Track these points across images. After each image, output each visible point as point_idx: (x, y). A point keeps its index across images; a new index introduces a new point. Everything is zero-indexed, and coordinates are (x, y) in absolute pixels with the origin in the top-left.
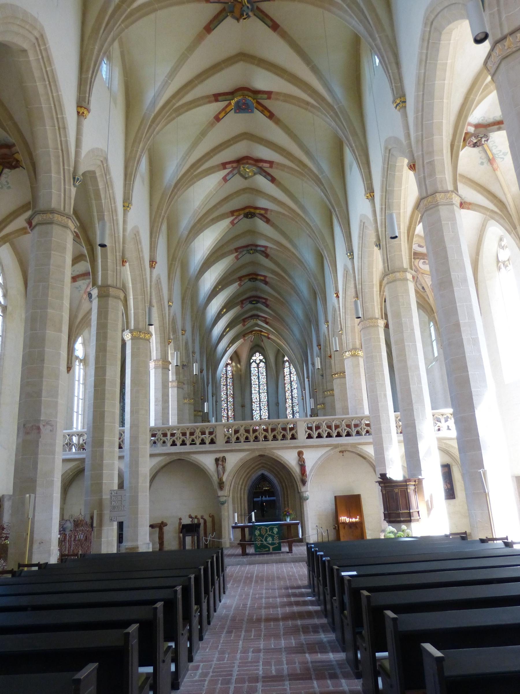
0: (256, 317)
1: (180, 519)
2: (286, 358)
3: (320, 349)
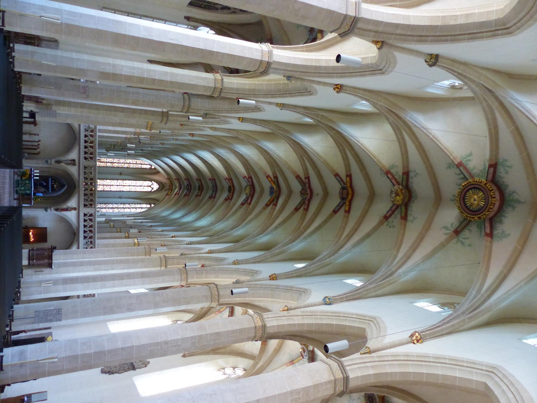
1: (38, 135)
2: (153, 205)
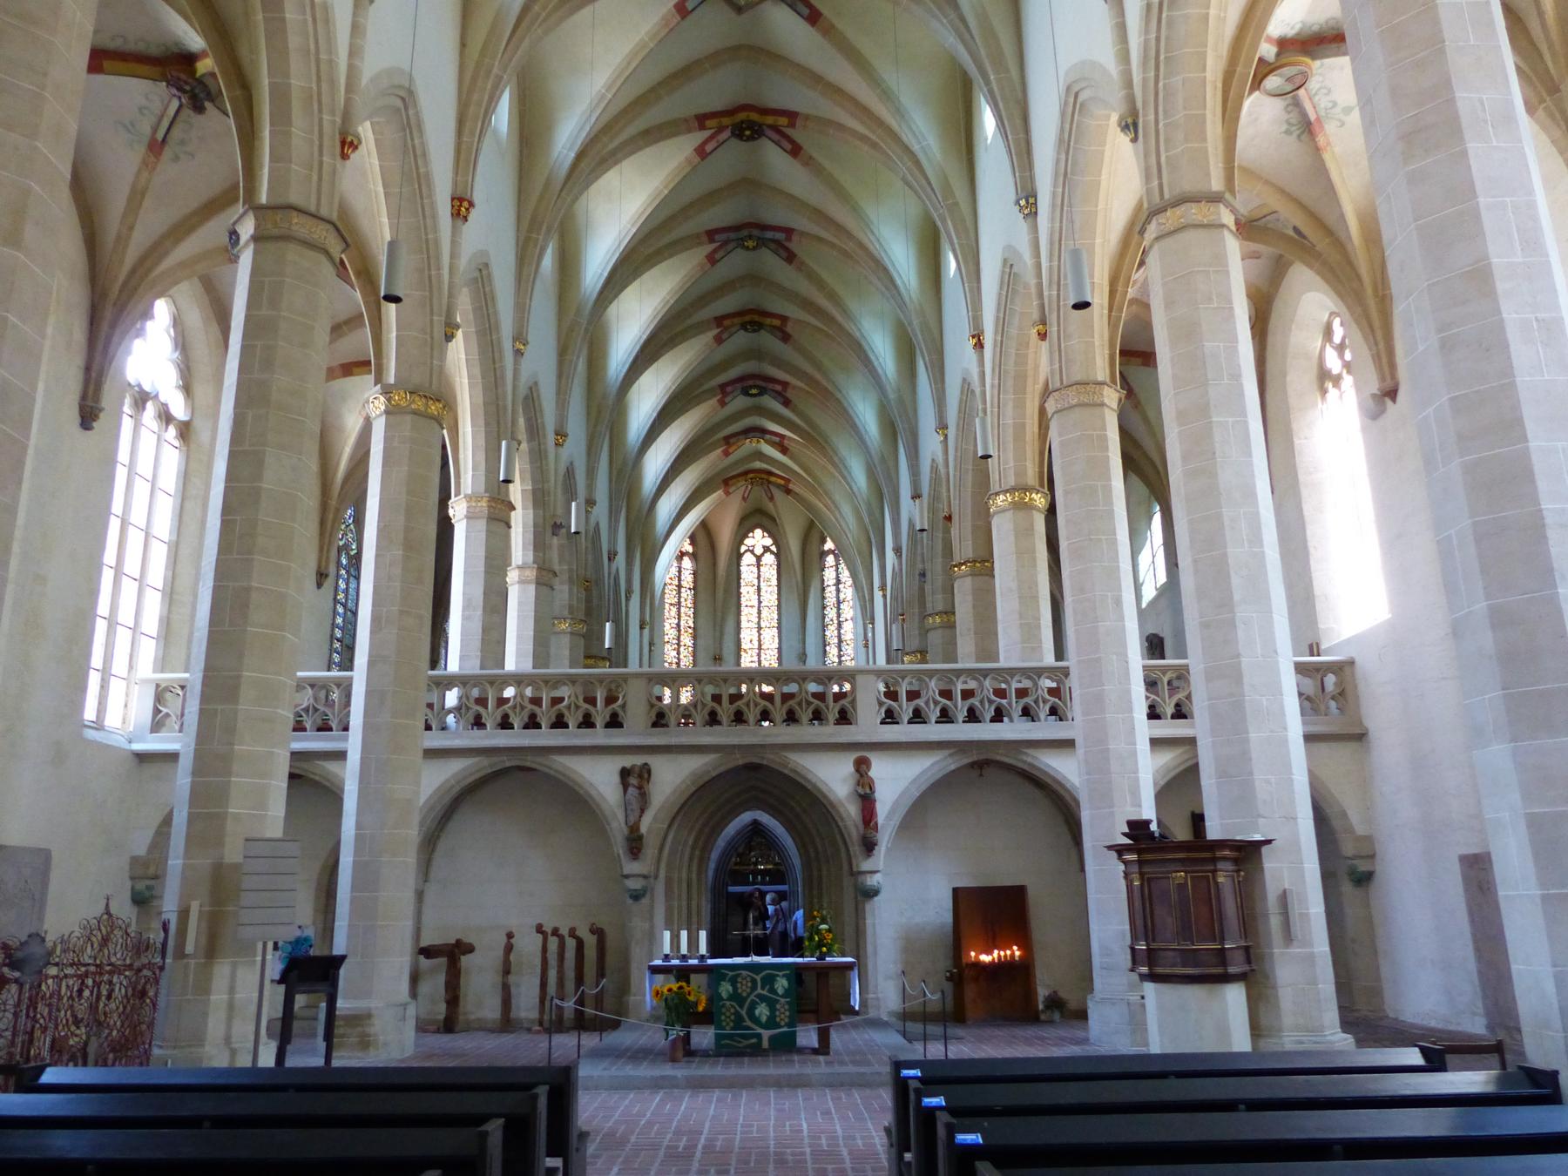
0: (758, 435)
2: (829, 545)
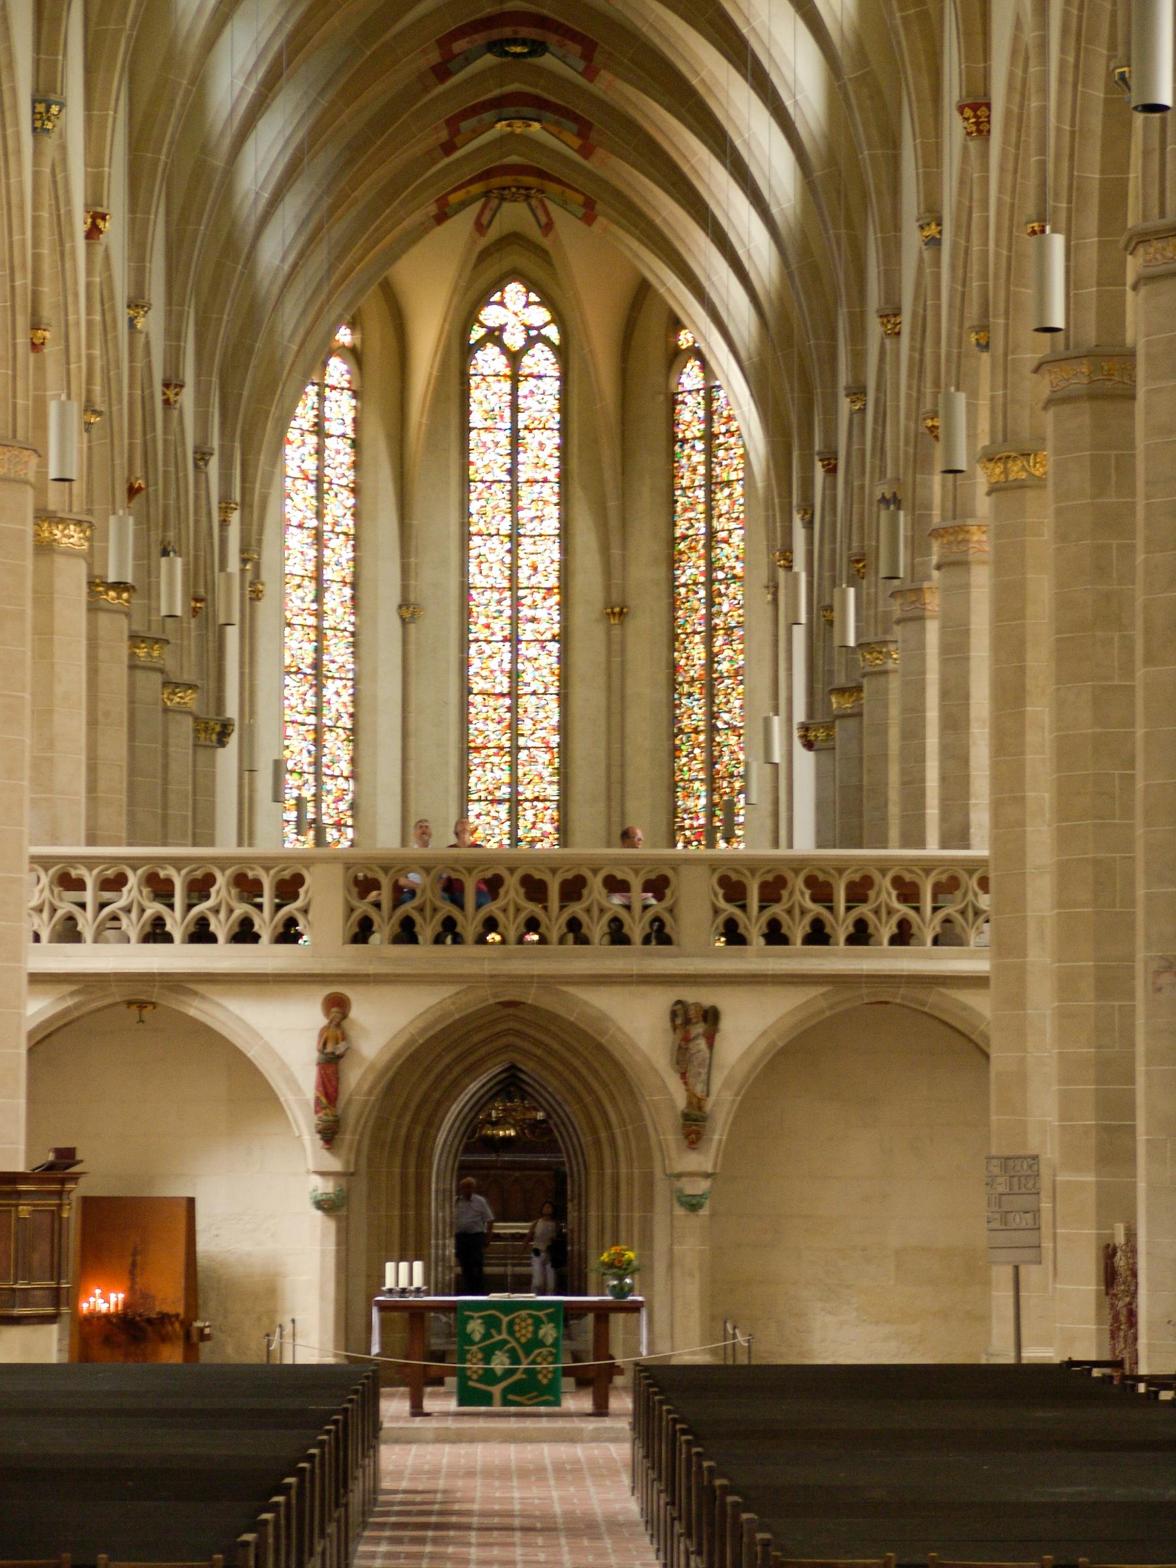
0: (526, 111)
3: (863, 411)
